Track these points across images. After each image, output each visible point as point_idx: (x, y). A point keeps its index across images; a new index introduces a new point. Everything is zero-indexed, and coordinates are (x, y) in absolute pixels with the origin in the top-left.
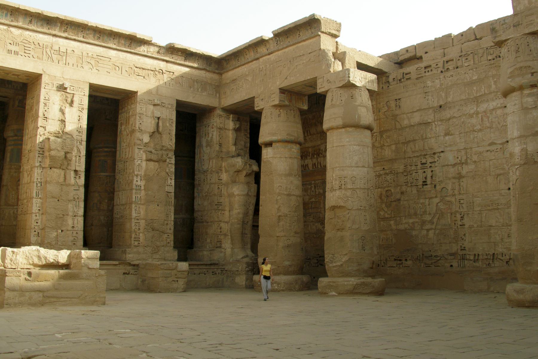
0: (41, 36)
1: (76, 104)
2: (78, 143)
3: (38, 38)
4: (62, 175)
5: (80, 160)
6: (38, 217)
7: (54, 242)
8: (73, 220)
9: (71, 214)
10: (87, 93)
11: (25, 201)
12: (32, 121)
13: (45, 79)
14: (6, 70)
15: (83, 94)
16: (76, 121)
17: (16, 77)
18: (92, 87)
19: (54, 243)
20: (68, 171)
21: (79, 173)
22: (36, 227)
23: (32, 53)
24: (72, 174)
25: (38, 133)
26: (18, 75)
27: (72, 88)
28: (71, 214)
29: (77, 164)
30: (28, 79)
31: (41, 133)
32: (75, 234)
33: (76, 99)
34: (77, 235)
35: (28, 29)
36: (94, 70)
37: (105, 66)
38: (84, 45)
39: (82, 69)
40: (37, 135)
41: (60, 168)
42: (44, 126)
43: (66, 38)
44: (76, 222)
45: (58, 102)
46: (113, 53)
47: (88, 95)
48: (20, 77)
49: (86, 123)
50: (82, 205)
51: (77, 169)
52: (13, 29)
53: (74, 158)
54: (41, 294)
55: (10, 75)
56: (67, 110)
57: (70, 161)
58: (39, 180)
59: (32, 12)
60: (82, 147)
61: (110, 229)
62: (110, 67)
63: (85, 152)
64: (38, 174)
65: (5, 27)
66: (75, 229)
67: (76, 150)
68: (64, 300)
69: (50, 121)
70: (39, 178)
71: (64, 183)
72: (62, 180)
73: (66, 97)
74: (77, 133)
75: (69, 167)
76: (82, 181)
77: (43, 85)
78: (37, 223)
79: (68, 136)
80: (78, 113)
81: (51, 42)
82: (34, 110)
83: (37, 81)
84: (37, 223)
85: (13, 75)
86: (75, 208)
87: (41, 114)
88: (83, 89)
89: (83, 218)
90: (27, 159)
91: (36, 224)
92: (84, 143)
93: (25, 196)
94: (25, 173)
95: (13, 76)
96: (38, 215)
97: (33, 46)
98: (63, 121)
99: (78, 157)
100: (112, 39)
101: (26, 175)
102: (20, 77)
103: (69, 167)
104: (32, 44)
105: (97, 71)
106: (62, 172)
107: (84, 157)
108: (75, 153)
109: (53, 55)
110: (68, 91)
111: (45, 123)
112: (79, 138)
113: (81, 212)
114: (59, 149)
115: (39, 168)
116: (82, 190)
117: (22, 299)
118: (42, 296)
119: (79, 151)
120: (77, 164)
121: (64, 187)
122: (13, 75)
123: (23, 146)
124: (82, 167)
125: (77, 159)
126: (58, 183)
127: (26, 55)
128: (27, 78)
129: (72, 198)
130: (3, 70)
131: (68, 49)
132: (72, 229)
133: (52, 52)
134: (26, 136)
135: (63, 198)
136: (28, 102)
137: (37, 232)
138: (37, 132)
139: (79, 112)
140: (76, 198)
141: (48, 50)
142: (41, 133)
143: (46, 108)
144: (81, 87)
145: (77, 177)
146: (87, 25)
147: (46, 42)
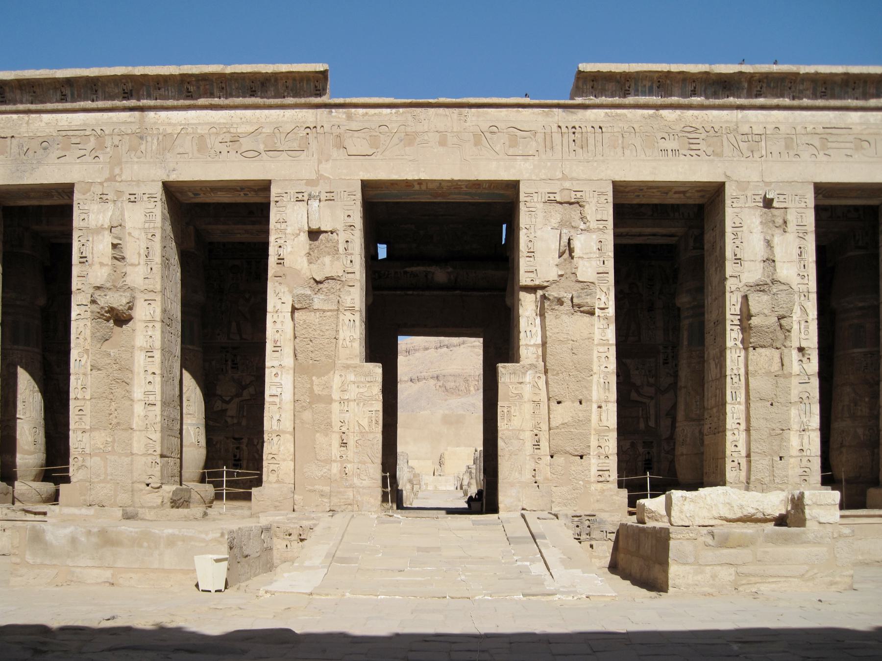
0: (715, 113)
1: (791, 227)
2: (802, 298)
3: (711, 118)
4: (777, 360)
5: (807, 327)
6: (737, 435)
7: (768, 479)
8: (801, 437)
9: (795, 426)
10: (811, 203)
11: (715, 410)
12: (716, 269)
13: (730, 191)
14: (662, 187)
15: (803, 205)
16: (795, 257)
17: (682, 195)
18: (820, 189)
19: (766, 480)
20: (786, 350)
21: (807, 352)
22: (735, 454)
23: (703, 146)
24: (795, 354)
25: (728, 288)
26: (684, 193)
27: (782, 197)
28: (795, 426)
29: (803, 336)
30: (703, 197)
31: (733, 288)
32: (805, 462)
33: (791, 217)
34: (809, 464)
35: (690, 107)
36: (821, 157)
37: (842, 145)
38: (797, 113)
39: (798, 159)
40: (724, 293)
41: (772, 346)
42: (737, 274)
43: (762, 108)
44: (806, 441)
45: (759, 228)
46: (855, 116)
47: (813, 205)
48: (688, 195)
49: (814, 259)
50: (816, 409)
51: (804, 344)
52: (664, 113)
53: (795, 326)
54: (732, 570)
55: (670, 194)
56: (777, 240)
57: (789, 331)
58: (735, 372)
59: (694, 74)
60: (809, 304)
61: (876, 450)
62: (852, 145)
63: (816, 313)
64: (732, 361)
65: (651, 112)
66: (804, 454)
67: (799, 311)
68: (774, 580)
69: (746, 264)
70: (735, 368)
71: (780, 373)
72: (776, 366)
73: (773, 216)
74: (799, 279)
75: (788, 343)
76: (813, 366)
77: (728, 202)
78: (736, 446)
79: (785, 287)
80: (797, 242)
81: (735, 120)
82: (718, 248)
83: (718, 196)
84: (736, 446)
85: (676, 193)
86: (803, 416)
87: (729, 254)
88: (803, 197)
89: (818, 434)
90: (713, 337)
91: (734, 449)
92: (814, 297)
93: (713, 402)
94: (711, 362)
95: (677, 196)
96: (736, 432)
97: (704, 135)
98: (770, 261)
99: (803, 323)
100: (850, 90)
101: (713, 365)
102: (688, 195)
103: (788, 343)
104: (702, 130)
105: (825, 158)
106: (776, 354)
107: (815, 322)
108: (797, 315)
109: (741, 144)
110: (775, 204)
111: (738, 269)
112: (803, 288)
113: (815, 421)
114: (766, 312)
115: (733, 351)
116: (815, 382)
117: (699, 577)
118: (734, 573)
119: (804, 310)
120: (803, 336)
121: (781, 380)
122: (676, 193)
123: (706, 316)
124: (812, 340)
125: (802, 327)
126: (768, 373)
127: (692, 153)
128: (700, 194)
129: (797, 399)
130: (658, 187)
131: (767, 126)
132: (798, 454)
133: (739, 138)
134: (710, 298)
135: (780, 400)
136: (708, 237)
137: (736, 463)
138: (725, 287)
139: (798, 240)
140: (804, 397)
141: (731, 137)
142: (733, 288)
143: (738, 242)
144: (800, 192)
145: (805, 359)
146: (798, 74)
147: (727, 122)
